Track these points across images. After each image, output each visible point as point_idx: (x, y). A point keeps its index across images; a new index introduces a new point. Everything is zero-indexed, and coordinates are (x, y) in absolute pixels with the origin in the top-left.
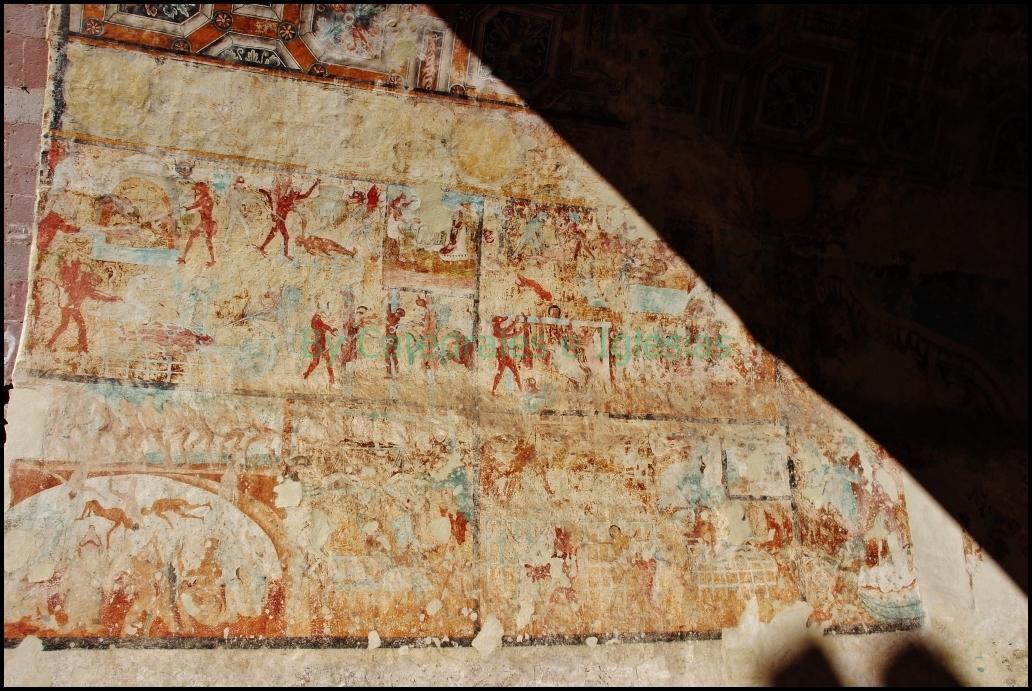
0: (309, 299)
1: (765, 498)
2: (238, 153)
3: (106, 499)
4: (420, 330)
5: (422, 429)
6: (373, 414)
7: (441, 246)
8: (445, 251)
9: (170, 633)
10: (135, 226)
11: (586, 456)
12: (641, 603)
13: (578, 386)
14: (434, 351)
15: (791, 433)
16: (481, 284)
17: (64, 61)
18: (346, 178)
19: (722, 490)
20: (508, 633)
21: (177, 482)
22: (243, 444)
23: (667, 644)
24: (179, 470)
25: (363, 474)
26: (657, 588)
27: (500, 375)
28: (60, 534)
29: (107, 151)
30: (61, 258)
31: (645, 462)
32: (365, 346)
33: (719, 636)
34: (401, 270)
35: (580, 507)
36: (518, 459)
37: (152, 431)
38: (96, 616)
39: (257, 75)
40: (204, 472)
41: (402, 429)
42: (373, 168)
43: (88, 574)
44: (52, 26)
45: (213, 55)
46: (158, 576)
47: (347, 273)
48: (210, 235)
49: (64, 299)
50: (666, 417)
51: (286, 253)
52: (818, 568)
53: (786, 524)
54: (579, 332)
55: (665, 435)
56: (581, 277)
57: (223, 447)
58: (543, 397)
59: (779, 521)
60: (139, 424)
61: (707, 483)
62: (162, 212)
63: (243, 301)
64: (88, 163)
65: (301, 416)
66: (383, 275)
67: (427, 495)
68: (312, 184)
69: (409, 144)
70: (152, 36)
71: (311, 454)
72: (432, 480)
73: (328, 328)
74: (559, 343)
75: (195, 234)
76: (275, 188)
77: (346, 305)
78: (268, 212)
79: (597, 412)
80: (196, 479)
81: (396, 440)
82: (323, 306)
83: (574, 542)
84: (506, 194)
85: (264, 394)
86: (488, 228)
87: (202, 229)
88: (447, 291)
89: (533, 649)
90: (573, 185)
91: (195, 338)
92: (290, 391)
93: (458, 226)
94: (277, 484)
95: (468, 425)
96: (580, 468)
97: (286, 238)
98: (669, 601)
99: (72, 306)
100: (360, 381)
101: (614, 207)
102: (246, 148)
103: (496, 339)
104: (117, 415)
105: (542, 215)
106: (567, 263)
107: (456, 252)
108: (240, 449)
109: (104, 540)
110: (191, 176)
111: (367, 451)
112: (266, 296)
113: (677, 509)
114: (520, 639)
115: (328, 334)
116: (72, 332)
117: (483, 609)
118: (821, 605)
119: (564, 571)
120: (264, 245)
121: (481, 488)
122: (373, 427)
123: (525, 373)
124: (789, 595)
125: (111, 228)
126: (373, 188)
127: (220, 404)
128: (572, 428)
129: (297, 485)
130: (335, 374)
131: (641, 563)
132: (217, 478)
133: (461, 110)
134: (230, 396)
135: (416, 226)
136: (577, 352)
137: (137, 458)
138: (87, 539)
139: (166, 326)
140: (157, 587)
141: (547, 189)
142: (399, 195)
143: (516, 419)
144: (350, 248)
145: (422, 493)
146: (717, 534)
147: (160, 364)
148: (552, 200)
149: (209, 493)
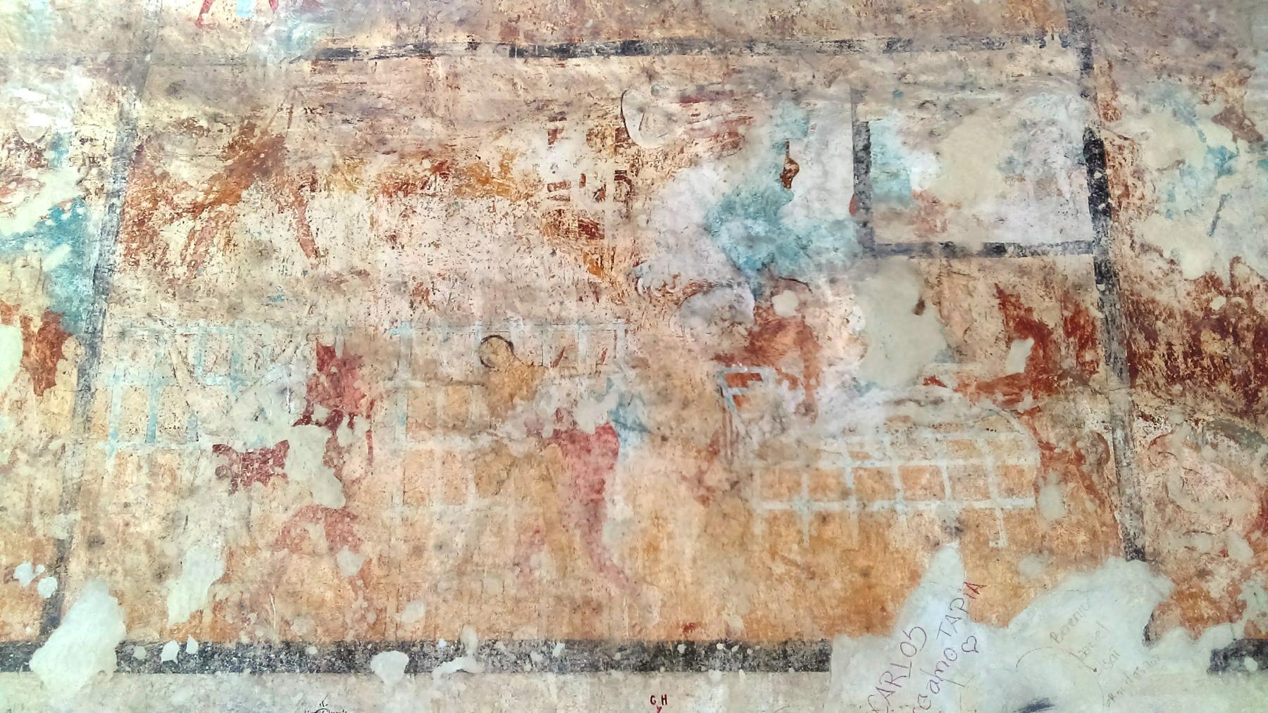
1: (999, 250)
12: (563, 553)
15: (1099, 63)
19: (851, 231)
20: (137, 634)
23: (638, 679)
26: (617, 509)
31: (607, 167)
33: (820, 661)
35: (400, 287)
36: (231, 171)
50: (683, 46)
52: (1189, 457)
53: (1075, 326)
55: (673, 91)
58: (330, 19)
59: (1049, 314)
61: (800, 214)
79: (473, 46)
83: (364, 383)
89: (205, 682)
95: (111, 98)
96: (405, 187)
98: (652, 548)
113: (704, 288)
114: (170, 652)
117: (76, 566)
118: (1203, 574)
119: (327, 462)
121: (120, 248)
124: (1082, 537)
128: (398, 87)
131: (570, 438)
143: (247, 76)
146: (826, 352)
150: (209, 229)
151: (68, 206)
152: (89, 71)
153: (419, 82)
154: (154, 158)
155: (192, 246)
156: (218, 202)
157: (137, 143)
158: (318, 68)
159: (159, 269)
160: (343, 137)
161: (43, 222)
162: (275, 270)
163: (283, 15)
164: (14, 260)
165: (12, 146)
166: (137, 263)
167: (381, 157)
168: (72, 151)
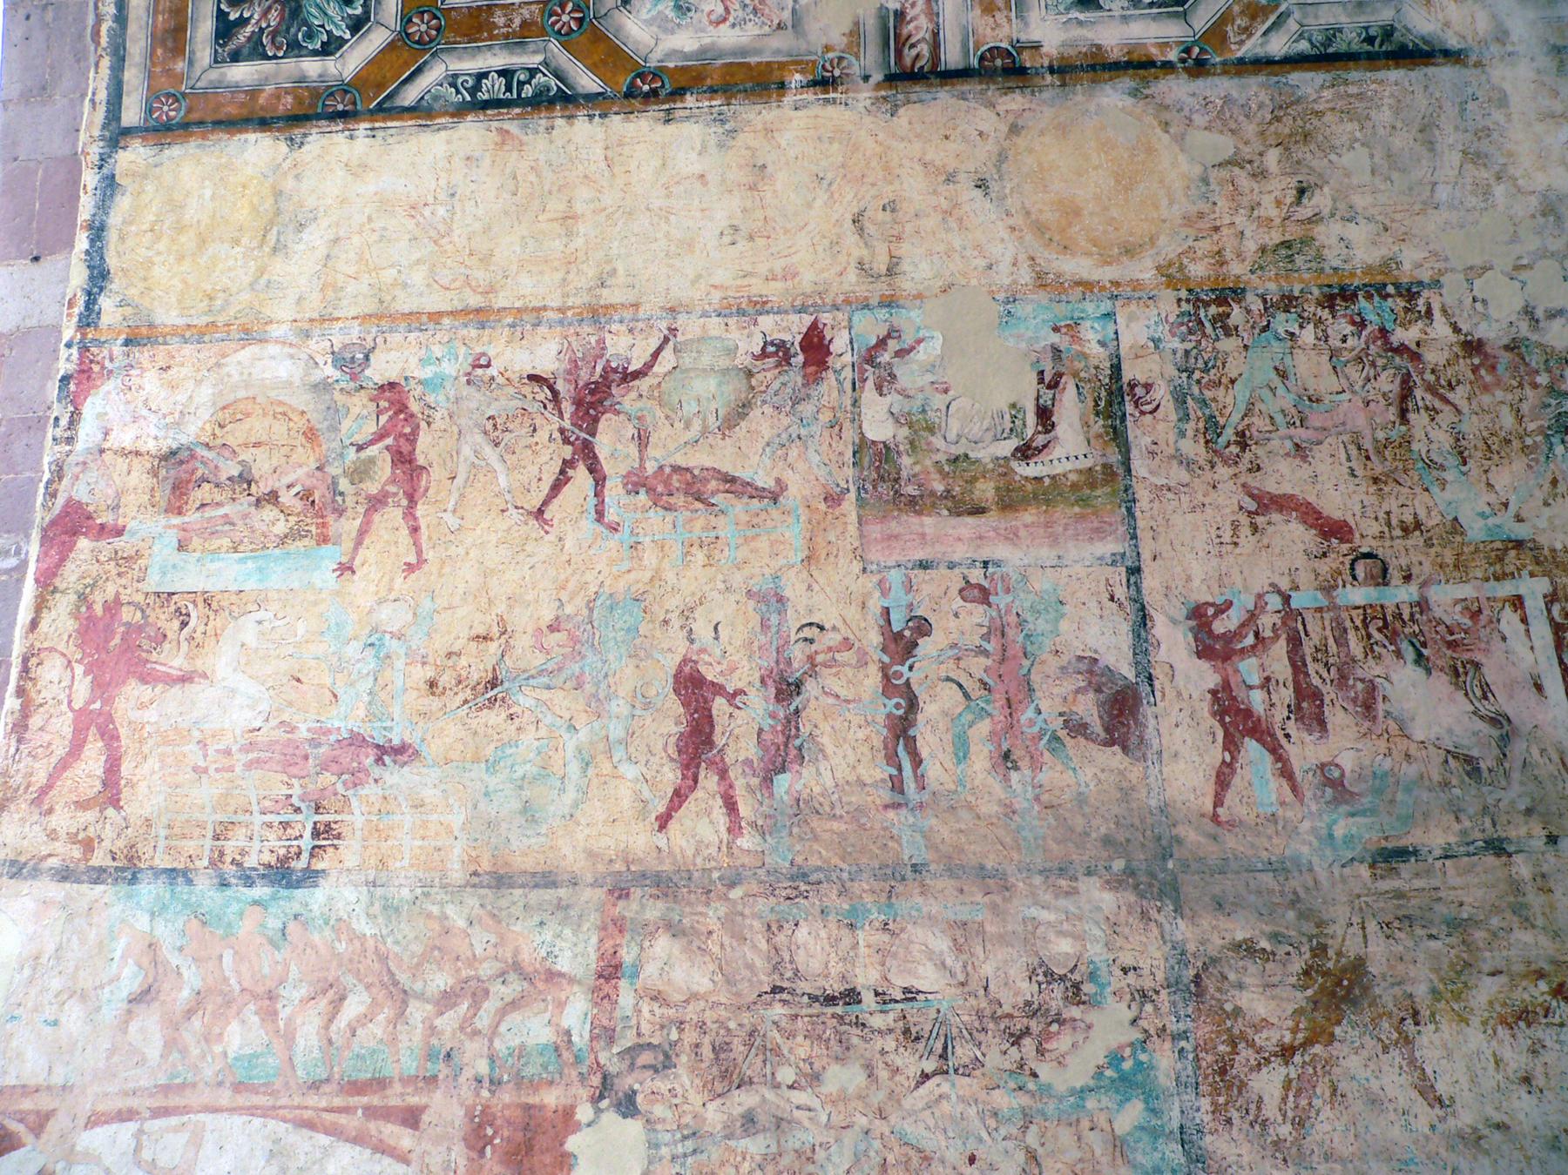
0: (666, 622)
2: (475, 301)
4: (978, 665)
5: (1002, 939)
6: (853, 910)
7: (1014, 443)
8: (1026, 452)
10: (245, 502)
11: (1540, 975)
13: (1478, 770)
14: (1023, 719)
16: (1141, 524)
17: (110, 185)
18: (741, 312)
21: (306, 1132)
22: (483, 1021)
24: (313, 1100)
25: (830, 1086)
27: (1230, 765)
29: (188, 349)
30: (82, 597)
32: (825, 727)
34: (914, 520)
37: (255, 997)
39: (507, 125)
40: (375, 1100)
41: (942, 944)
42: (807, 280)
44: (90, 124)
45: (406, 103)
47: (763, 544)
48: (412, 499)
49: (83, 688)
51: (600, 515)
54: (1457, 617)
56: (1430, 464)
57: (432, 1030)
58: (1373, 811)
60: (226, 980)
62: (301, 469)
63: (493, 648)
64: (150, 383)
65: (647, 931)
66: (861, 536)
67: (1032, 1139)
68: (654, 343)
69: (890, 207)
70: (277, 96)
71: (674, 1036)
72: (1046, 1091)
73: (718, 689)
74: (1398, 654)
75: (377, 502)
76: (566, 365)
77: (764, 625)
78: (550, 425)
80: (351, 1122)
81: (927, 978)
82: (703, 632)
84: (1171, 282)
85: (546, 880)
86: (1141, 378)
87: (392, 489)
88: (1046, 554)
90: (1356, 232)
91: (372, 752)
92: (619, 866)
93: (1054, 385)
94: (577, 1127)
95: (1144, 915)
97: (600, 480)
99: (97, 705)
100: (815, 823)
101: (1486, 269)
102: (491, 290)
103: (1204, 665)
104: (175, 960)
105: (1283, 323)
106: (1381, 435)
107: (1057, 452)
108: (476, 1033)
110: (368, 372)
111: (841, 1019)
112: (553, 628)
115: (719, 705)
116: (93, 761)
120: (546, 503)
121: (1205, 1103)
122: (855, 945)
123: (1305, 751)
125: (192, 517)
126: (814, 326)
127: (429, 916)
128: (1480, 893)
129: (634, 1127)
130: (744, 810)
132: (411, 1118)
133: (1015, 102)
134: (455, 892)
135: (938, 401)
136: (1457, 675)
137: (208, 1072)
139: (303, 727)
141: (1283, 252)
142: (883, 332)
143: (1294, 883)
144: (765, 481)
145: (1014, 1131)
147: (285, 825)
148: (1304, 282)
149: (387, 1160)
150: (1306, 1077)
151: (1128, 1052)
152: (1108, 882)
153: (1503, 886)
154: (1219, 990)
155: (1291, 1099)
156: (1309, 1042)
157: (1192, 972)
158: (1379, 872)
159: (1257, 1128)
160: (1435, 957)
161: (1102, 1073)
162: (1397, 1126)
163: (1314, 808)
164: (1078, 1121)
165: (1041, 978)
166: (1229, 1121)
167: (1489, 980)
168: (1115, 985)
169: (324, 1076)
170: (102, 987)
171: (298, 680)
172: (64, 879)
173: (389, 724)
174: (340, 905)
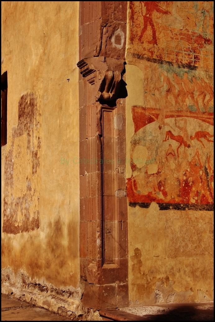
3: (174, 130)
9: (209, 203)
24: (204, 116)
28: (157, 148)
37: (190, 93)
38: (178, 193)
43: (172, 170)
46: (201, 173)
99: (148, 16)
104: (173, 83)
109: (176, 152)
116: (149, 32)
137: (185, 108)
138: (169, 152)
139: (190, 31)
140: (201, 179)
147: (189, 55)
169: (205, 111)
170: (161, 87)
171: (189, 18)
172: (149, 61)
173: (206, 34)
174: (201, 75)
